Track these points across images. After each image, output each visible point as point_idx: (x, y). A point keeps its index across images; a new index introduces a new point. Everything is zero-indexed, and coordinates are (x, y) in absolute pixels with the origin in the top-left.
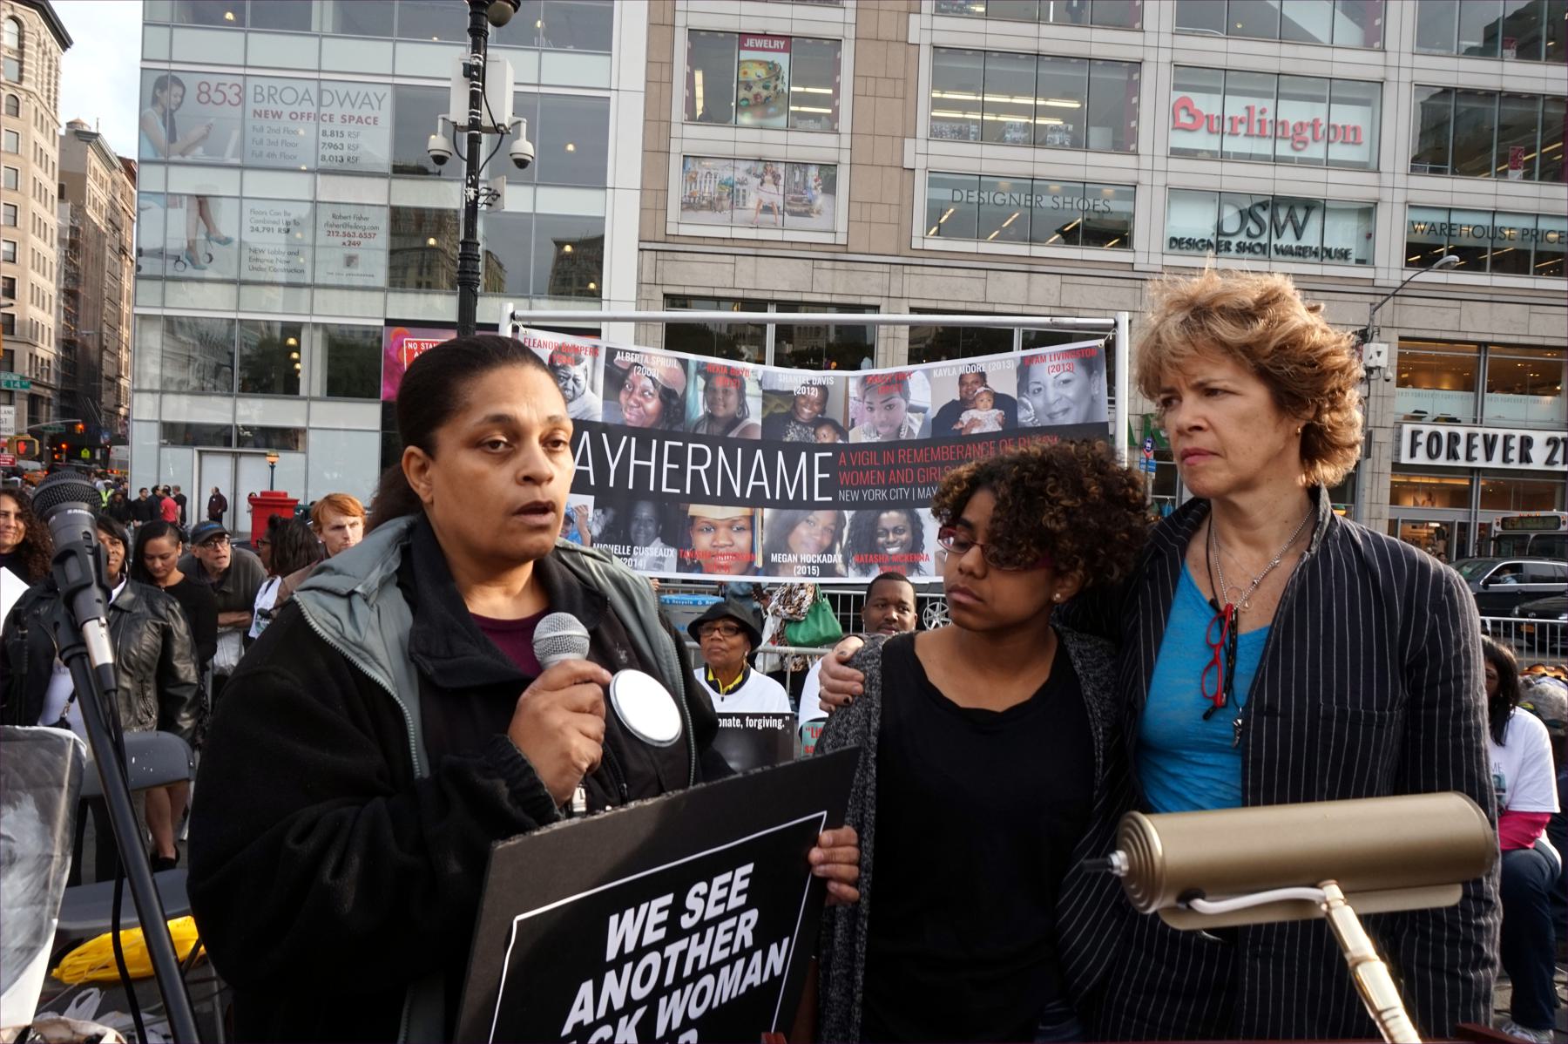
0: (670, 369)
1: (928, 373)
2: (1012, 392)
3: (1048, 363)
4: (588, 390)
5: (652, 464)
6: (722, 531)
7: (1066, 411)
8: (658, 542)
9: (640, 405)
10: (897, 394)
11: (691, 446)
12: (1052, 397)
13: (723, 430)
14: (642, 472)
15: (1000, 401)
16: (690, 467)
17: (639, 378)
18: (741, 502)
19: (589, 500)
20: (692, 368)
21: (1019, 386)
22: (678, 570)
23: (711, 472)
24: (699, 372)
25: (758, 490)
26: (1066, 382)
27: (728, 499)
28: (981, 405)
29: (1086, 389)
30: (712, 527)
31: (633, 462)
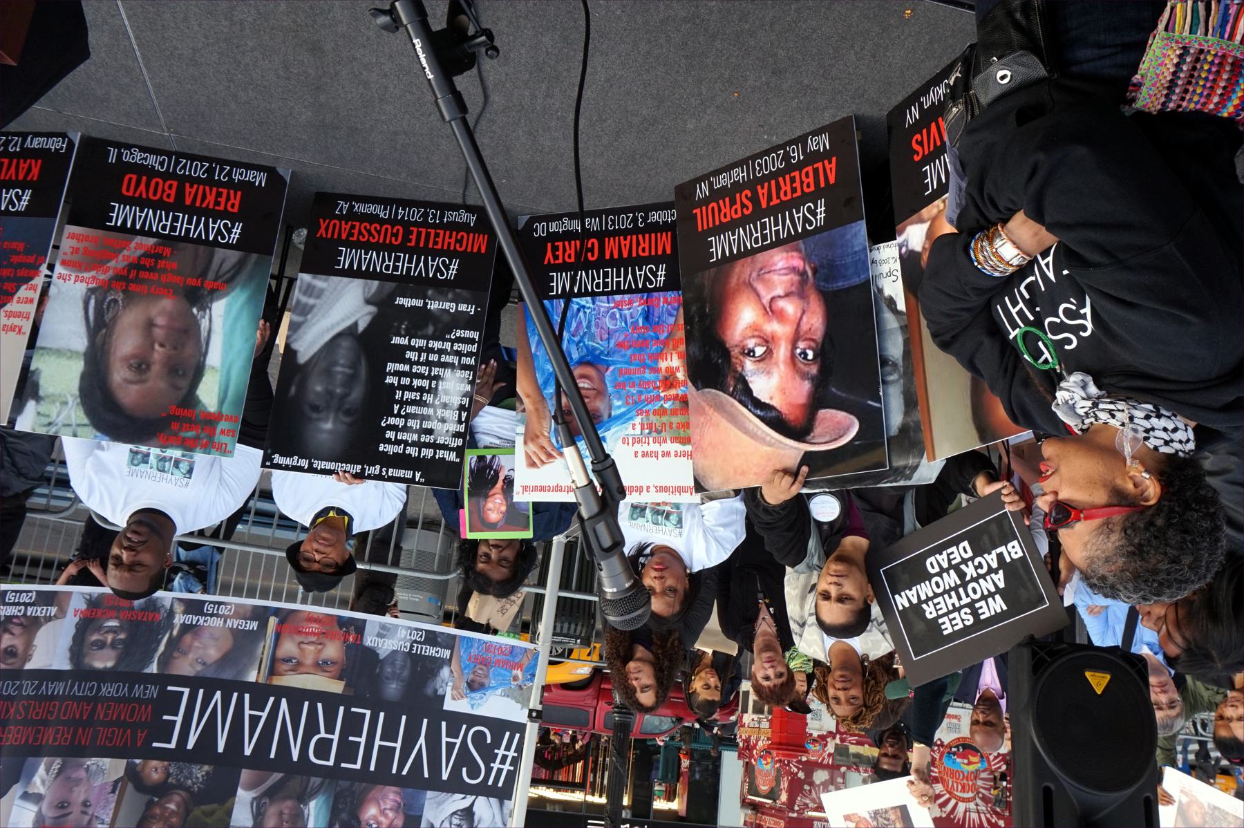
11: (331, 763)
16: (336, 737)
23: (312, 728)
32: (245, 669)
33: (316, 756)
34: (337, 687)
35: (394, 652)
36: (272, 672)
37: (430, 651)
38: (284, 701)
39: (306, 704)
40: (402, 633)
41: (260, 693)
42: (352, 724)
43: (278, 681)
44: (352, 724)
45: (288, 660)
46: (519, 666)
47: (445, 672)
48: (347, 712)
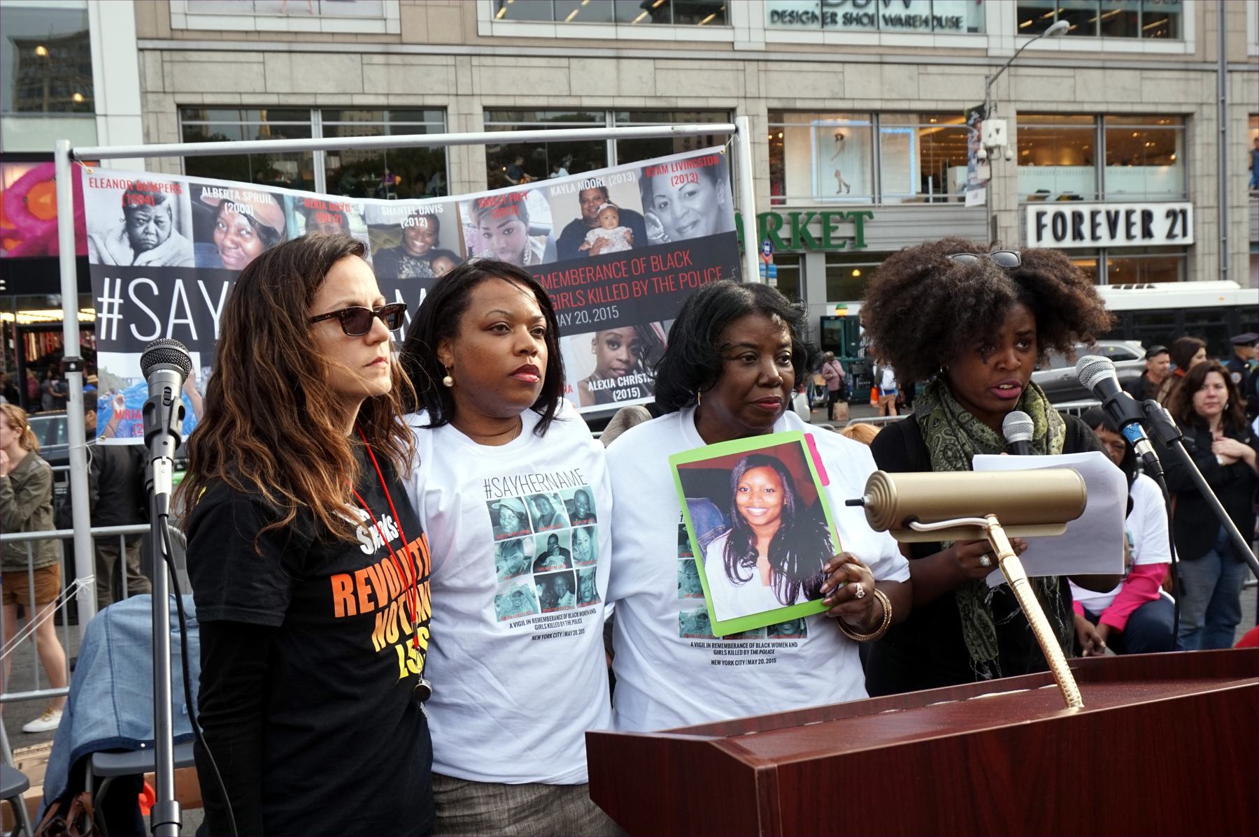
0: (266, 205)
1: (545, 191)
2: (638, 208)
3: (670, 174)
4: (175, 233)
7: (694, 224)
10: (514, 217)
12: (679, 211)
15: (625, 217)
17: (232, 216)
20: (289, 204)
21: (644, 200)
24: (296, 208)
26: (692, 194)
28: (607, 222)
29: (712, 199)
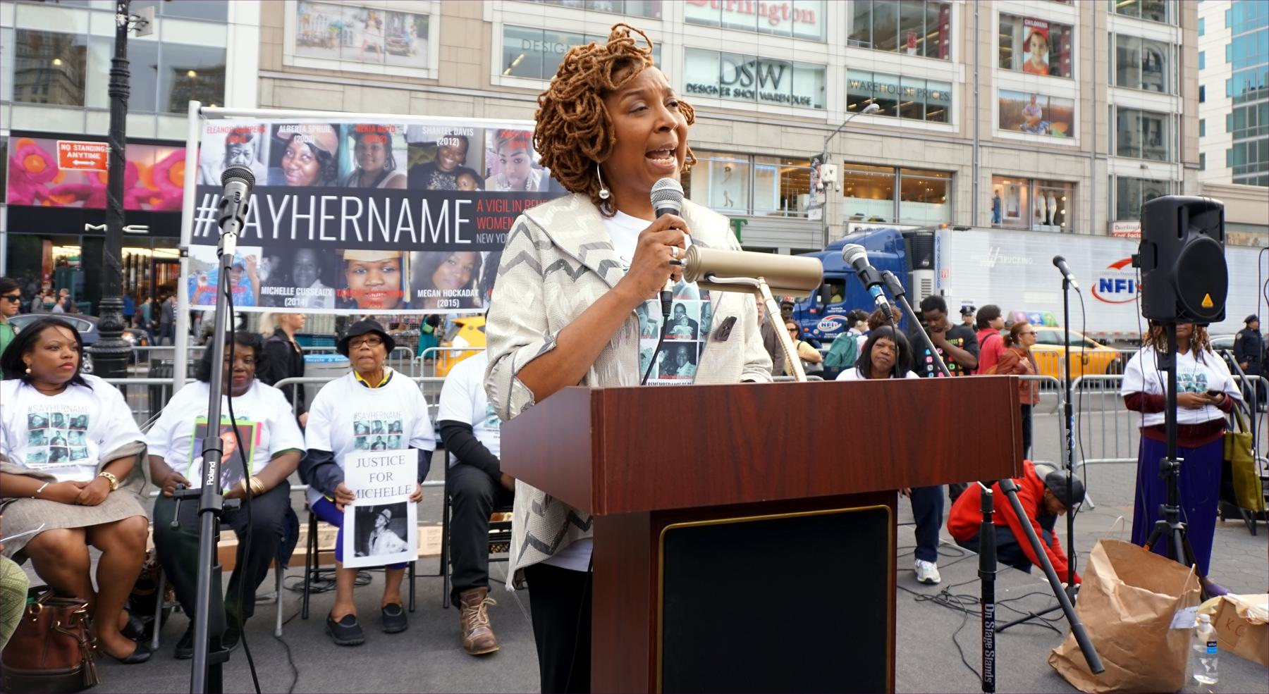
5: (311, 217)
6: (374, 272)
8: (318, 283)
9: (300, 167)
11: (345, 199)
13: (371, 185)
14: (303, 224)
16: (344, 217)
18: (390, 246)
19: (257, 251)
22: (337, 307)
23: (363, 222)
25: (405, 235)
27: (379, 244)
30: (365, 269)
31: (295, 216)
32: (420, 259)
33: (356, 203)
34: (349, 254)
35: (308, 286)
36: (400, 260)
37: (279, 291)
38: (387, 239)
39: (370, 239)
40: (304, 302)
41: (405, 243)
42: (333, 228)
43: (394, 254)
44: (333, 228)
45: (390, 270)
46: (202, 290)
47: (264, 276)
48: (338, 236)
